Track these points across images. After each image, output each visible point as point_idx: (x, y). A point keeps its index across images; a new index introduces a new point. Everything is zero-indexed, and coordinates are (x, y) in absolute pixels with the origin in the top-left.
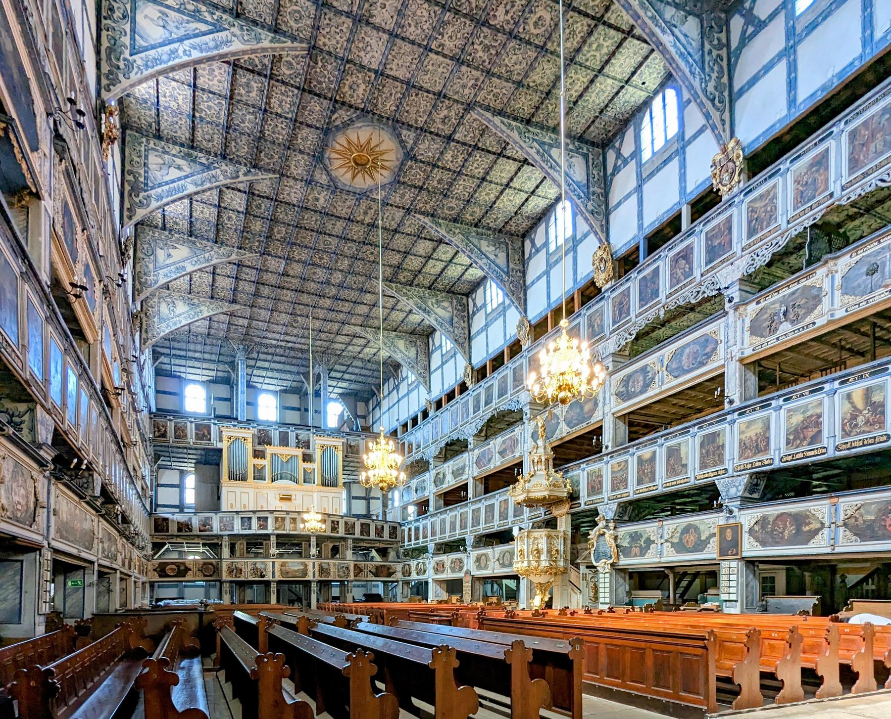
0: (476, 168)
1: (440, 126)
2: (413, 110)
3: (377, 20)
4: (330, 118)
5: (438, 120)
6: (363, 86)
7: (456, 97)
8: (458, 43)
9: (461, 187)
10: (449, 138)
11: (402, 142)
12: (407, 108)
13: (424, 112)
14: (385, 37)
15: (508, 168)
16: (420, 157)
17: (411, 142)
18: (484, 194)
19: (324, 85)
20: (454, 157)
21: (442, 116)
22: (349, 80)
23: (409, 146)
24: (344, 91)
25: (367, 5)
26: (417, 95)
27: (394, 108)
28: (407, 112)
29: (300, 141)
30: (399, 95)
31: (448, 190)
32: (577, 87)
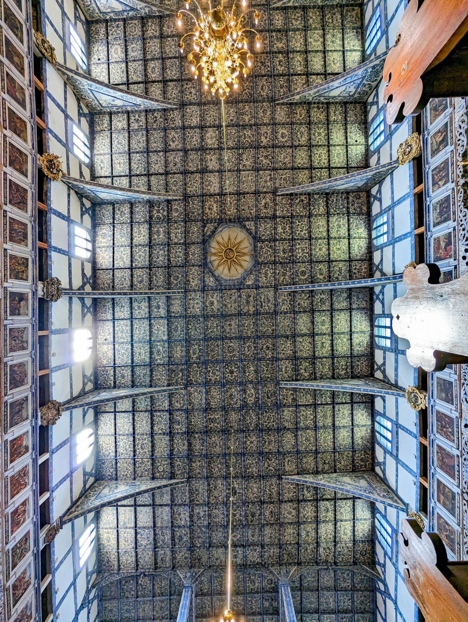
0: (301, 231)
1: (265, 211)
2: (246, 208)
3: (210, 168)
4: (203, 231)
5: (262, 208)
6: (215, 205)
7: (265, 190)
8: (251, 160)
9: (300, 251)
10: (274, 217)
11: (248, 230)
12: (243, 208)
13: (253, 206)
14: (217, 174)
15: (320, 223)
16: (263, 238)
17: (254, 228)
18: (317, 250)
19: (196, 214)
20: (284, 228)
21: (263, 204)
22: (207, 204)
23: (253, 231)
24: (206, 212)
25: (204, 163)
26: (244, 197)
27: (235, 211)
28: (243, 210)
29: (191, 256)
30: (235, 202)
31: (293, 255)
32: (324, 157)
